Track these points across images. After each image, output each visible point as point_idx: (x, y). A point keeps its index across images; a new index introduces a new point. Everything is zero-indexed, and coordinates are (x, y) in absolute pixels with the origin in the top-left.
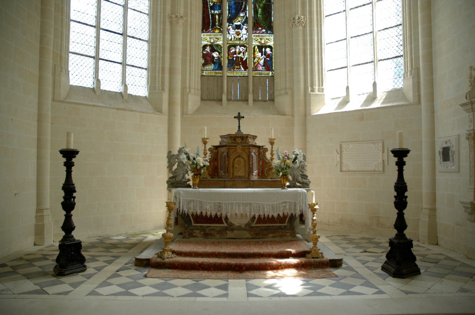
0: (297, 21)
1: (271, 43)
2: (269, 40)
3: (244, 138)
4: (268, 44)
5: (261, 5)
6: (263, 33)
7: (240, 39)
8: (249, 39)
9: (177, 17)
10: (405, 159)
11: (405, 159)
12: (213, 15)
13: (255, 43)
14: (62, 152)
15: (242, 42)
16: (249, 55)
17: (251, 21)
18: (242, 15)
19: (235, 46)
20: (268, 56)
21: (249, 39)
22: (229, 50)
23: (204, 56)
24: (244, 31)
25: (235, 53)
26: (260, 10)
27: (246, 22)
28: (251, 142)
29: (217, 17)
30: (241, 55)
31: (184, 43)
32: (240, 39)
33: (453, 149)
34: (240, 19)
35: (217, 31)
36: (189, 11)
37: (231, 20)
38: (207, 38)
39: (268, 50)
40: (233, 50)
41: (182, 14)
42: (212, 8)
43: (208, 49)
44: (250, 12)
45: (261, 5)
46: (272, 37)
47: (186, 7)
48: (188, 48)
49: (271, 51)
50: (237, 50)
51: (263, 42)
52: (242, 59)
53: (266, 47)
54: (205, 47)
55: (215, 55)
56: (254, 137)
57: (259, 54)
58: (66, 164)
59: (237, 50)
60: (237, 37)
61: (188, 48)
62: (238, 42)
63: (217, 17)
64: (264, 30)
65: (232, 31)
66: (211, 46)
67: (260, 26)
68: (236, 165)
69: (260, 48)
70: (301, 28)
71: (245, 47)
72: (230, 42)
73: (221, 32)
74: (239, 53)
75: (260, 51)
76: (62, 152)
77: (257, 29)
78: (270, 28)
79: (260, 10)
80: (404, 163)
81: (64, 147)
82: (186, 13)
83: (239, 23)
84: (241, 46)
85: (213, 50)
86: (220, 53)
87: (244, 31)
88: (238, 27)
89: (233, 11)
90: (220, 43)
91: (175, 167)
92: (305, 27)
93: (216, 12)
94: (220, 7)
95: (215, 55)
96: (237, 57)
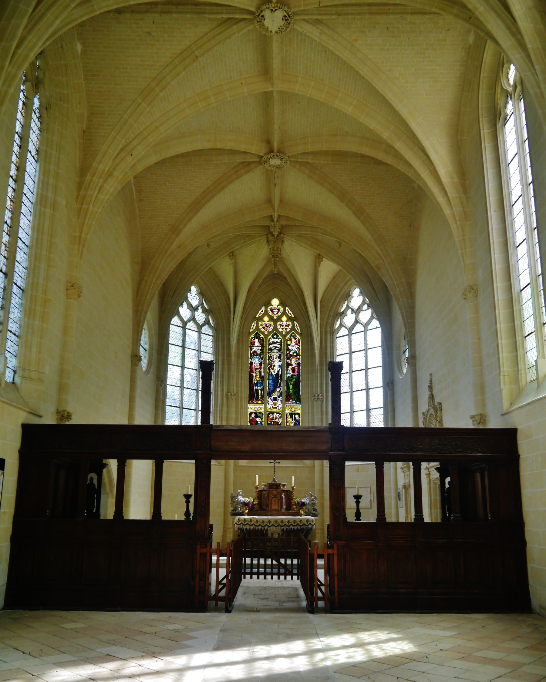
0: (316, 398)
1: (299, 412)
2: (298, 408)
3: (278, 486)
4: (297, 412)
5: (292, 382)
6: (293, 403)
7: (276, 408)
8: (284, 408)
9: (231, 395)
10: (360, 500)
11: (360, 500)
12: (257, 390)
13: (287, 411)
14: (184, 495)
15: (278, 411)
16: (283, 420)
17: (284, 395)
18: (278, 390)
19: (272, 413)
20: (297, 421)
21: (284, 408)
22: (268, 416)
23: (251, 421)
24: (279, 402)
25: (273, 418)
26: (291, 386)
27: (281, 395)
28: (282, 488)
29: (260, 391)
30: (277, 420)
31: (236, 412)
32: (276, 408)
33: (401, 493)
34: (276, 393)
35: (260, 402)
36: (240, 389)
37: (270, 394)
38: (252, 408)
39: (297, 416)
40: (271, 417)
41: (235, 392)
42: (257, 385)
43: (253, 416)
44: (283, 388)
45: (292, 382)
46: (299, 407)
47: (237, 387)
48: (239, 416)
49: (299, 417)
50: (274, 417)
51: (293, 410)
52: (278, 423)
53: (295, 414)
54: (251, 414)
55: (258, 420)
56: (284, 485)
57: (290, 420)
58: (186, 502)
59: (274, 417)
60: (274, 406)
61: (239, 416)
62: (275, 410)
63: (260, 391)
64: (294, 402)
65: (271, 403)
66: (255, 413)
67: (291, 399)
68: (273, 502)
69: (291, 414)
70: (320, 402)
71: (280, 414)
72: (269, 410)
73: (262, 403)
74: (276, 418)
75: (291, 417)
76: (184, 495)
77: (289, 401)
78: (298, 400)
79: (291, 386)
80: (360, 502)
81: (185, 493)
82: (237, 391)
83: (276, 396)
84: (277, 413)
85: (257, 416)
86: (261, 419)
87: (279, 402)
88: (275, 399)
89: (272, 387)
90: (262, 411)
91: (234, 504)
92: (322, 402)
93: (259, 388)
94: (262, 384)
95: (258, 420)
96: (274, 422)
